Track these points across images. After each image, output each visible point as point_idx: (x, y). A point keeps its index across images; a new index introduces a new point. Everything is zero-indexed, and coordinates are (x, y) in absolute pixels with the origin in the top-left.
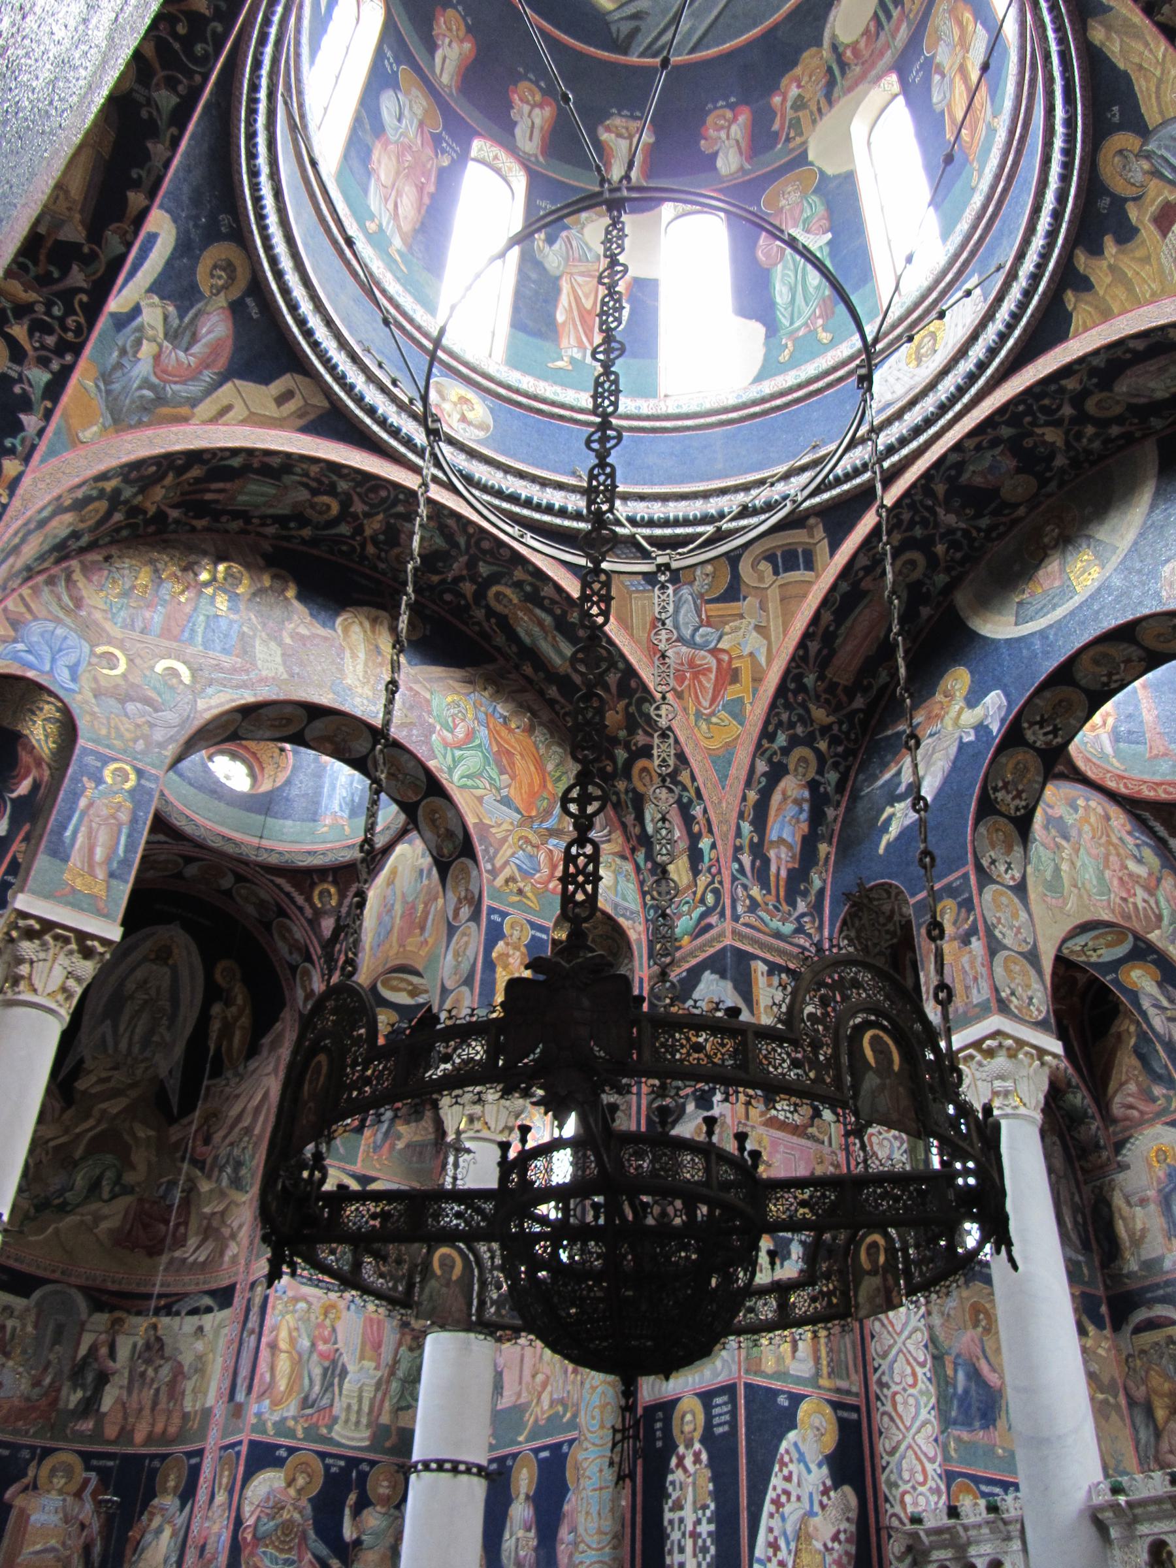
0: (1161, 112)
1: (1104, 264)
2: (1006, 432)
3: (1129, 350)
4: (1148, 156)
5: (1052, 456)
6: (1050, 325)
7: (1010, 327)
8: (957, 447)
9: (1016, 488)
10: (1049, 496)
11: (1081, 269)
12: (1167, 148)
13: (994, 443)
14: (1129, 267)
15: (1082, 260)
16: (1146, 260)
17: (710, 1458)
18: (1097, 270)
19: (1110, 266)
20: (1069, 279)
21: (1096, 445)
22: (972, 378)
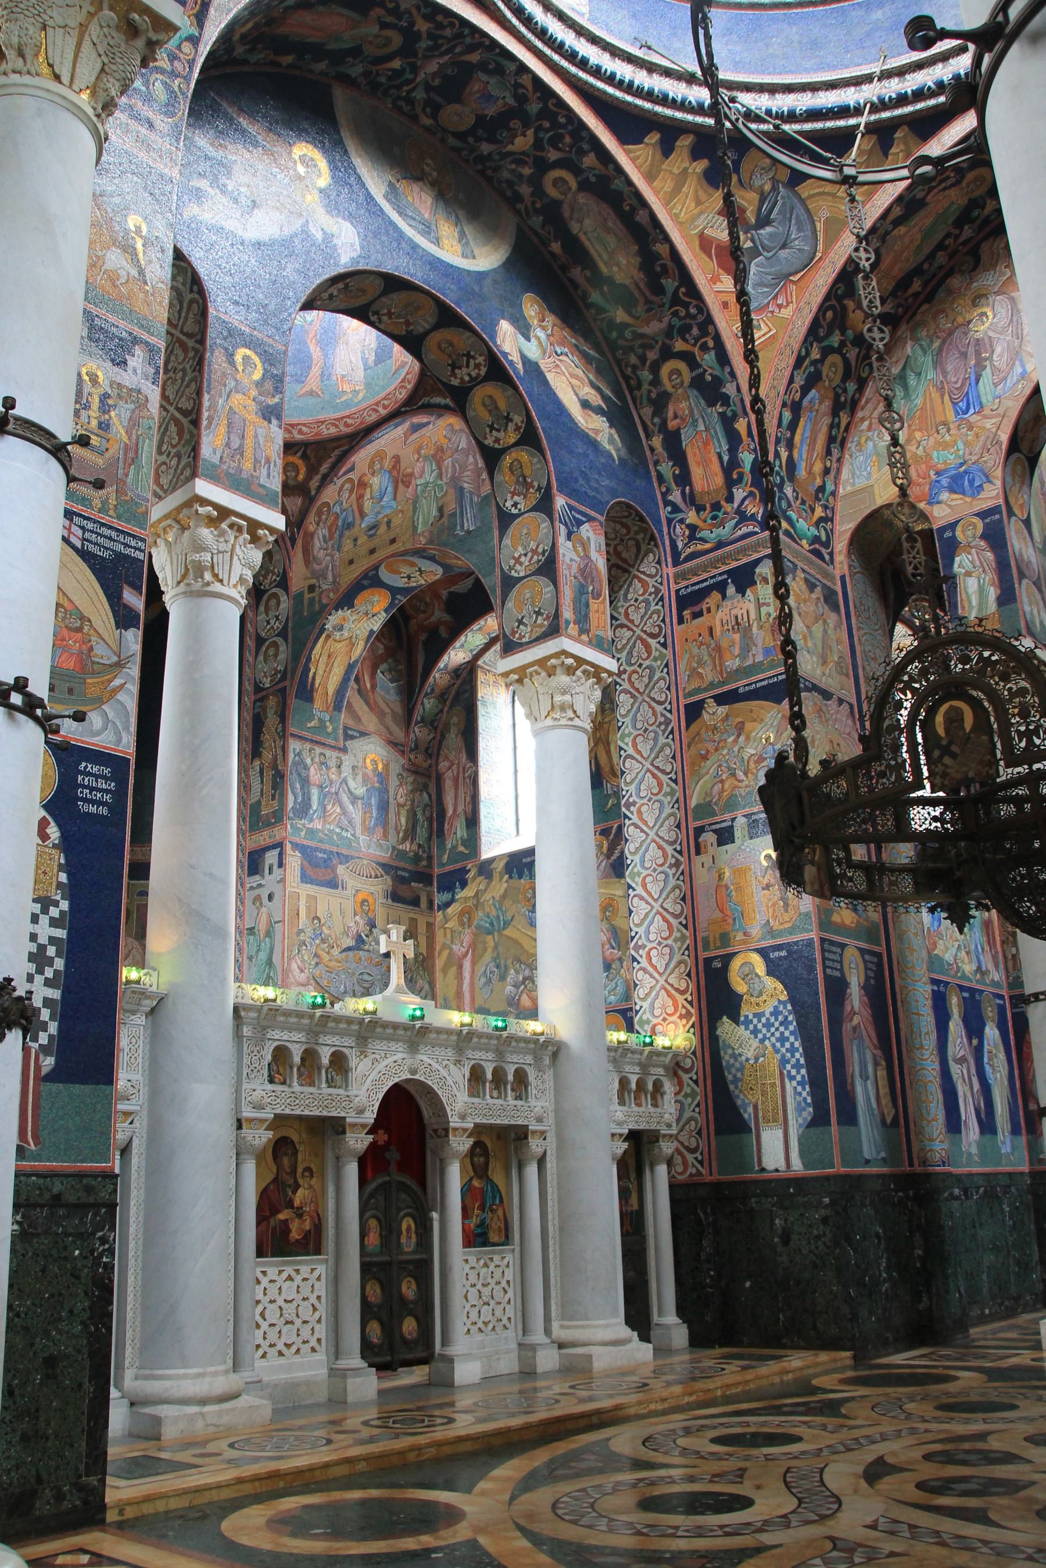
0: (810, 197)
1: (686, 164)
2: (534, 108)
3: (633, 209)
4: (774, 189)
5: (492, 140)
6: (629, 124)
7: (620, 85)
8: (523, 68)
9: (458, 116)
10: (443, 141)
11: (678, 143)
12: (784, 204)
13: (522, 99)
14: (691, 187)
15: (685, 142)
16: (698, 202)
17: (64, 837)
18: (680, 160)
19: (686, 169)
20: (670, 133)
21: (506, 175)
22: (572, 56)
